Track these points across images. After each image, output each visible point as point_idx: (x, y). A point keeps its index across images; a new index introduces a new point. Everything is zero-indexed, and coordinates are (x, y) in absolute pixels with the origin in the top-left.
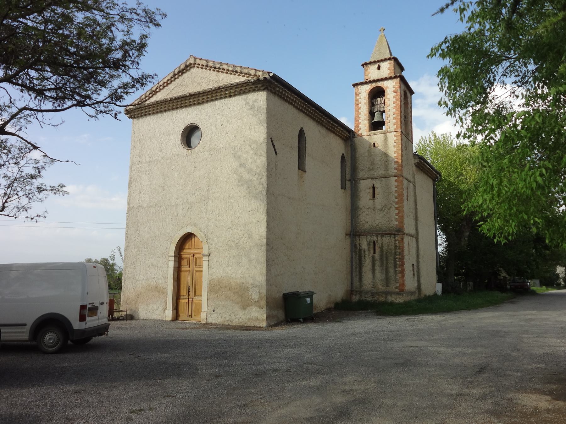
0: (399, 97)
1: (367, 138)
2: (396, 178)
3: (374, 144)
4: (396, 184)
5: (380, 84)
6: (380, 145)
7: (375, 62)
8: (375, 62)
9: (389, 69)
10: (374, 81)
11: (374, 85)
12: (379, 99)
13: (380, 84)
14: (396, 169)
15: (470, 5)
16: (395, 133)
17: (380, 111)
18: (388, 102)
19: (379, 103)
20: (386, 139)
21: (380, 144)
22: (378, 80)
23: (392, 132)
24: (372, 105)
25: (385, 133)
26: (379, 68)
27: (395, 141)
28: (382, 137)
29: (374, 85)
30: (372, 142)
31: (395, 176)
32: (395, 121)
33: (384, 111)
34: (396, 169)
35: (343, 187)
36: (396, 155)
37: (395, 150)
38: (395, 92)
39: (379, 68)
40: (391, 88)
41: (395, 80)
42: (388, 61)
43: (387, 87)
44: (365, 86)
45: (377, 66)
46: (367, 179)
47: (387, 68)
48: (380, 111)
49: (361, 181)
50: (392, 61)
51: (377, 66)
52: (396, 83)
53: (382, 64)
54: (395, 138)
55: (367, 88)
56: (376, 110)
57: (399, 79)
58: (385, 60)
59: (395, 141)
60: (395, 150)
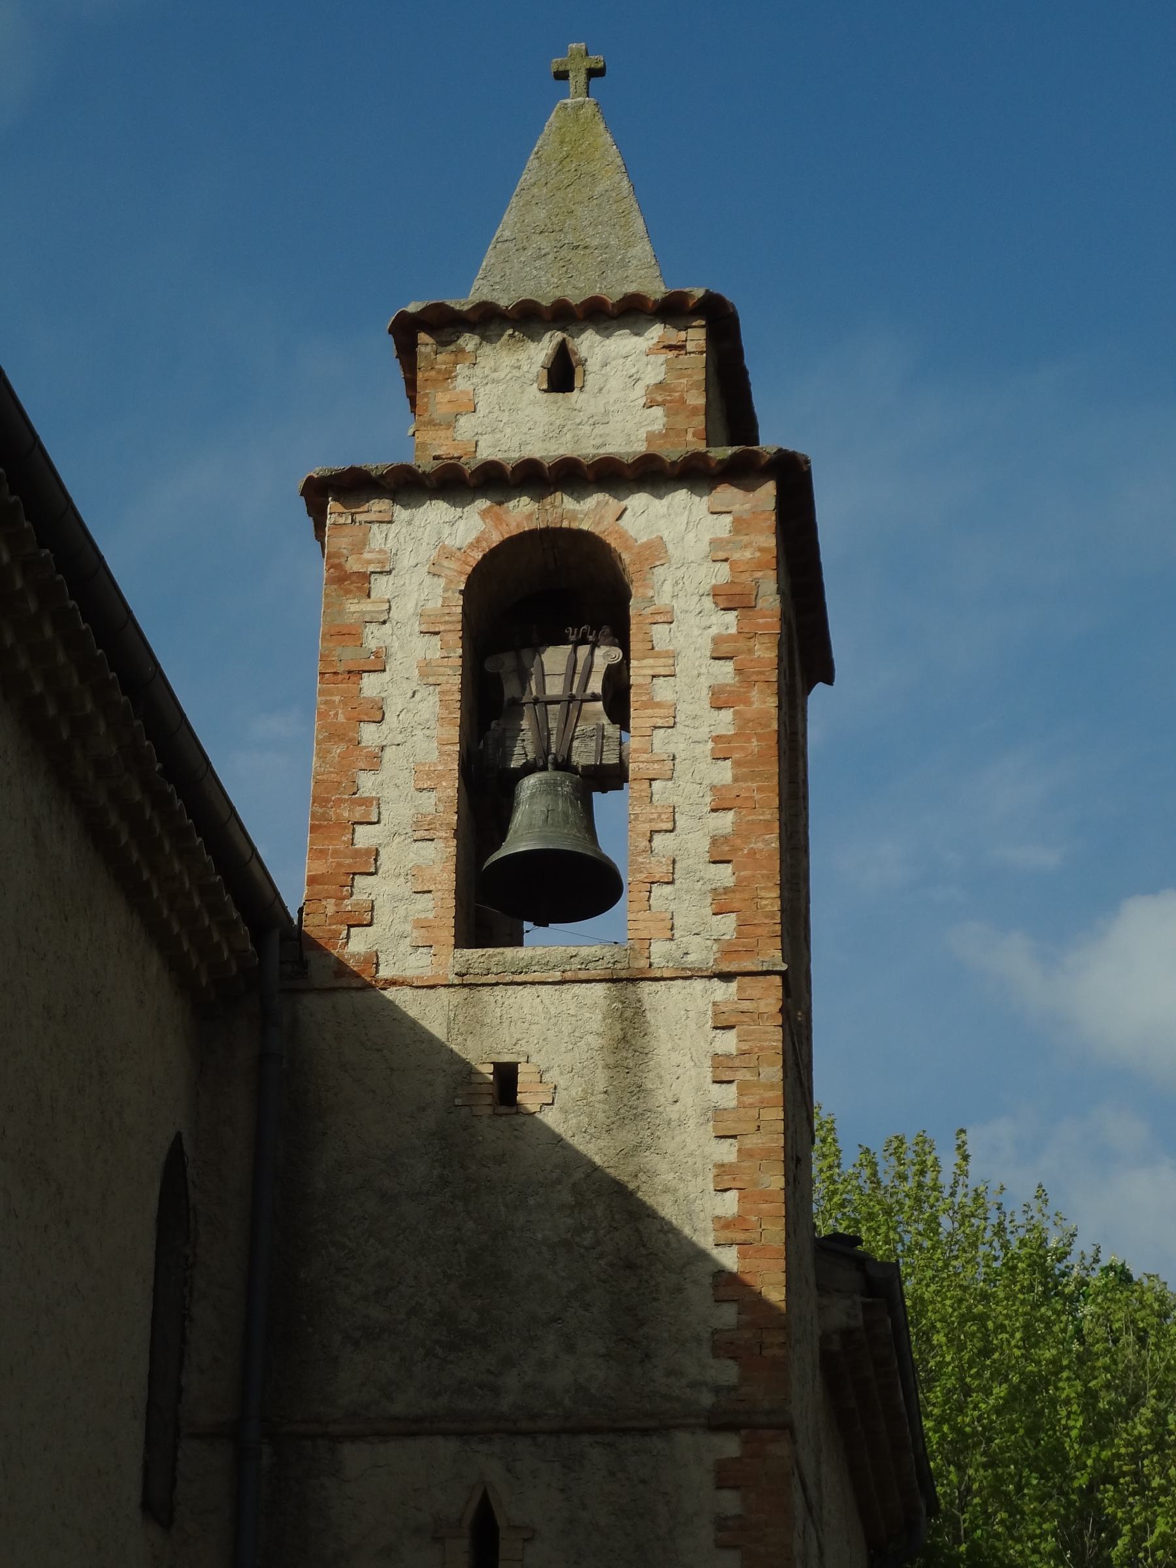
0: (766, 653)
1: (432, 1013)
2: (730, 1446)
3: (507, 1074)
4: (730, 1502)
5: (586, 512)
6: (571, 1089)
7: (528, 318)
8: (528, 318)
9: (658, 395)
10: (534, 478)
11: (523, 513)
12: (554, 658)
13: (586, 512)
14: (723, 1346)
15: (516, 1133)
16: (723, 992)
17: (564, 765)
18: (664, 691)
19: (555, 687)
20: (629, 1038)
21: (563, 1097)
22: (572, 476)
23: (688, 975)
24: (488, 705)
25: (625, 979)
26: (562, 375)
27: (720, 1062)
28: (595, 1021)
29: (523, 513)
30: (481, 1055)
31: (718, 1423)
32: (724, 875)
33: (612, 777)
34: (723, 1346)
35: (158, 1506)
36: (729, 1205)
37: (727, 1152)
38: (731, 599)
39: (562, 375)
40: (688, 554)
41: (727, 494)
42: (657, 332)
43: (655, 552)
44: (436, 512)
45: (540, 351)
46: (413, 1428)
47: (632, 389)
48: (564, 765)
49: (354, 1456)
50: (696, 337)
51: (540, 351)
52: (740, 526)
53: (590, 346)
54: (728, 1042)
55: (461, 531)
56: (523, 751)
57: (768, 490)
58: (630, 312)
59: (720, 1062)
60: (727, 1152)
